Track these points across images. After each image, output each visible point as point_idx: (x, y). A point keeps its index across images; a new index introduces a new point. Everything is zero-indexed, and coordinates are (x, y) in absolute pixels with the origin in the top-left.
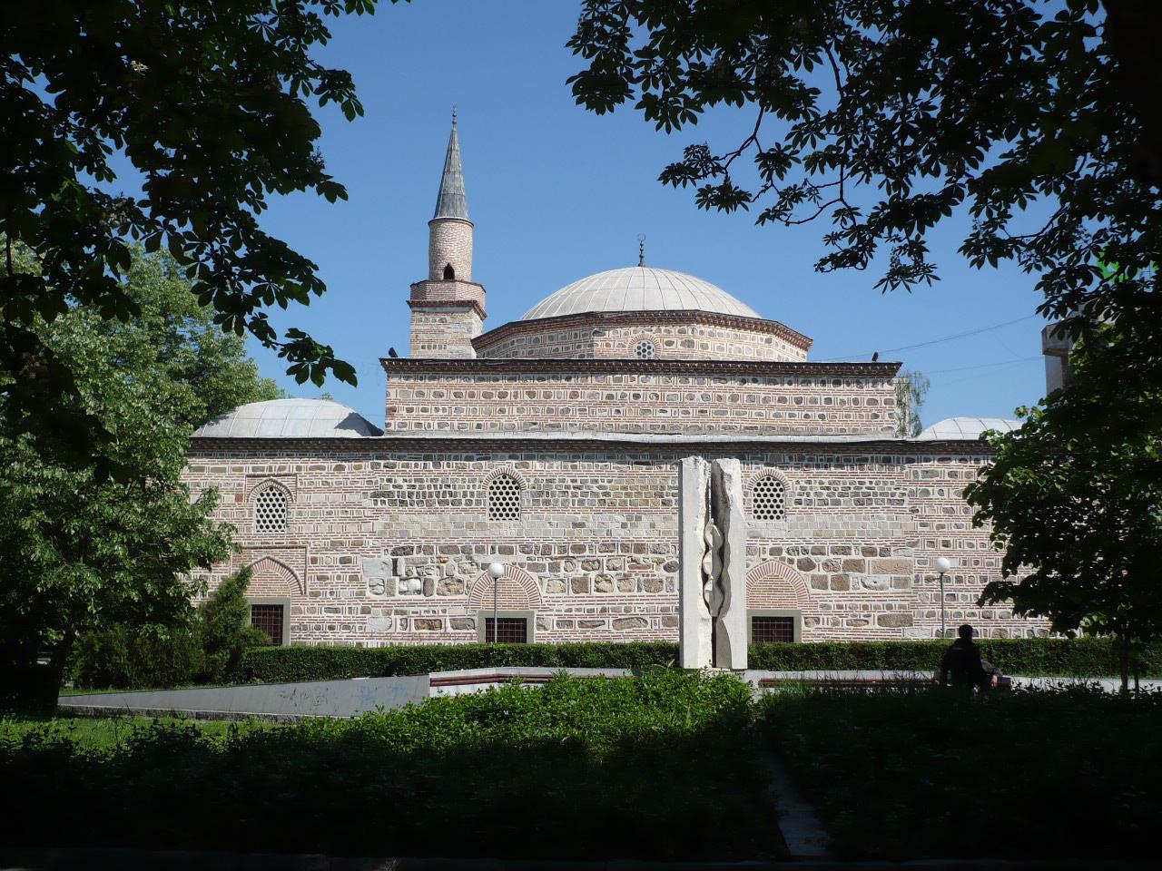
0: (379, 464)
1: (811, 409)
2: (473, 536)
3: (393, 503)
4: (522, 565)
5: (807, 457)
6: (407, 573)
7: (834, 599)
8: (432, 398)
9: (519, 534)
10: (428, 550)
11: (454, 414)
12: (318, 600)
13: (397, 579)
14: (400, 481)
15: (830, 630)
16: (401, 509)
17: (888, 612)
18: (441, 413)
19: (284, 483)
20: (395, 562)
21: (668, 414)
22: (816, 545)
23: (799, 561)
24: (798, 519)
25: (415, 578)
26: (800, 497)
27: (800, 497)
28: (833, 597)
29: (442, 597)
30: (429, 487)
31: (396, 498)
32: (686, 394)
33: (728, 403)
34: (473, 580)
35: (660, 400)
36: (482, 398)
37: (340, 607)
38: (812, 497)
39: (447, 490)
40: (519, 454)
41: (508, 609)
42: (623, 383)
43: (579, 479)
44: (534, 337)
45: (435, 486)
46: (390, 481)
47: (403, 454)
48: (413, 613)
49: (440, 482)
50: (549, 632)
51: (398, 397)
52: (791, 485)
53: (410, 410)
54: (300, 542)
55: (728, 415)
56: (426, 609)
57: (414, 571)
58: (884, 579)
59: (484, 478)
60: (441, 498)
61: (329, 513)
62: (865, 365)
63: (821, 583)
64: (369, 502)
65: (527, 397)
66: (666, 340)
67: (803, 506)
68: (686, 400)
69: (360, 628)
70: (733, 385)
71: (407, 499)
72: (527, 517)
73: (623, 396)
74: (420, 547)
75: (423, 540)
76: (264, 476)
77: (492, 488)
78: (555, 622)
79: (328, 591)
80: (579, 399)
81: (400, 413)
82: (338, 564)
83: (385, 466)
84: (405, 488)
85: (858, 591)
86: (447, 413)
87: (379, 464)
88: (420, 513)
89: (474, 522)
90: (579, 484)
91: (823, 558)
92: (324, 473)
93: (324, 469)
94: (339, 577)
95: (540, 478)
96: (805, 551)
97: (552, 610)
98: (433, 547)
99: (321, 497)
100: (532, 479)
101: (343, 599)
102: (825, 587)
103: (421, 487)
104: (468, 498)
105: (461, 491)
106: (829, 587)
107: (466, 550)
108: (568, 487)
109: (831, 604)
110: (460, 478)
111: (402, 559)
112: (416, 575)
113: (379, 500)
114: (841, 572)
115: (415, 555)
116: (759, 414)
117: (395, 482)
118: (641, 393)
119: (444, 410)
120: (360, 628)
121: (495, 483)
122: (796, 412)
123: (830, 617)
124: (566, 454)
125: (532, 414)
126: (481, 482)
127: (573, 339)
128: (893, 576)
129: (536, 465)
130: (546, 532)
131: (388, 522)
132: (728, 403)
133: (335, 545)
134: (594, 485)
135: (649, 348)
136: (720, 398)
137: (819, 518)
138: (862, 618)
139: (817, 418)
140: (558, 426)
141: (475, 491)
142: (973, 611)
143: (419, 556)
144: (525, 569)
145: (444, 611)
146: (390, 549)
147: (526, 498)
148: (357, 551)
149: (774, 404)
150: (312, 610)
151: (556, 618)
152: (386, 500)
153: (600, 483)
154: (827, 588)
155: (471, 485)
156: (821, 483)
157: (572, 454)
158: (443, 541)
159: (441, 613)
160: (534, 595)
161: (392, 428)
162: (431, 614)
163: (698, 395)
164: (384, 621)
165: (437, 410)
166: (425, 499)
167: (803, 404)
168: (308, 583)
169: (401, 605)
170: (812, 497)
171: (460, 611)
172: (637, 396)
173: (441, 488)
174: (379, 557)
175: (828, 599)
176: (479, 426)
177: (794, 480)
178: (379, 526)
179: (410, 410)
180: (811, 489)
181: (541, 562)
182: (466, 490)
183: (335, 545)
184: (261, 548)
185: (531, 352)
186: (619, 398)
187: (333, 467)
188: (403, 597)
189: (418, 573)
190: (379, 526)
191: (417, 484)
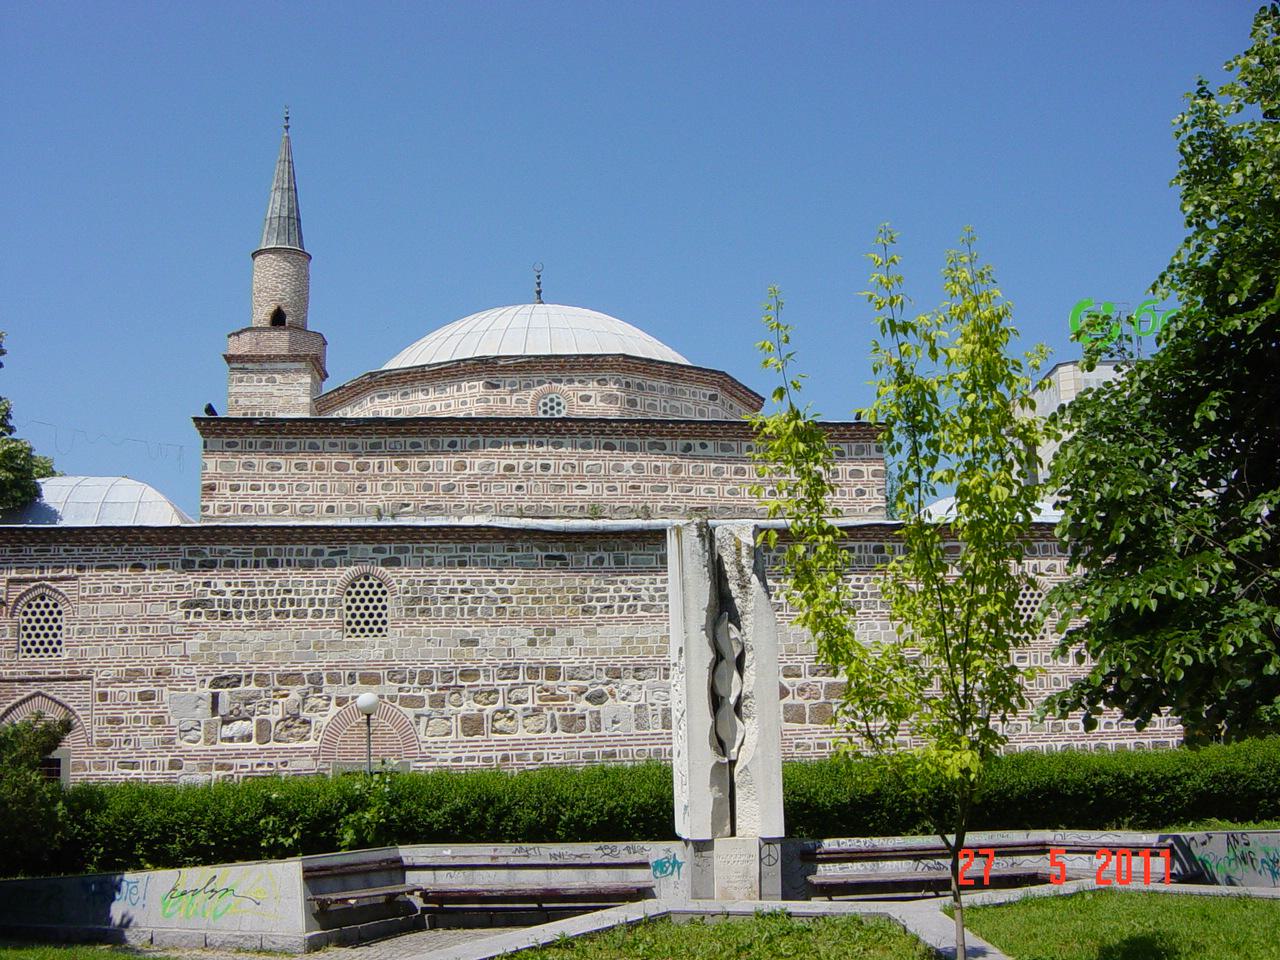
0: (193, 562)
3: (212, 615)
4: (392, 699)
7: (813, 736)
8: (265, 471)
9: (388, 654)
10: (262, 679)
11: (295, 492)
12: (109, 751)
14: (221, 585)
16: (224, 623)
18: (277, 491)
19: (61, 590)
20: (215, 697)
21: (588, 491)
22: (789, 664)
32: (612, 463)
33: (668, 476)
35: (576, 473)
36: (334, 471)
39: (287, 596)
40: (387, 546)
46: (207, 584)
48: (242, 767)
49: (276, 587)
54: (82, 670)
56: (259, 761)
60: (279, 608)
61: (124, 630)
62: (847, 425)
65: (396, 469)
66: (580, 394)
68: (612, 472)
72: (394, 635)
73: (528, 467)
74: (249, 676)
75: (255, 668)
76: (34, 580)
80: (467, 471)
81: (222, 491)
84: (228, 596)
86: (286, 492)
87: (193, 562)
90: (468, 585)
91: (799, 682)
94: (137, 719)
97: (434, 760)
99: (112, 608)
100: (405, 581)
102: (803, 721)
104: (317, 607)
107: (316, 681)
108: (454, 591)
109: (810, 742)
110: (305, 580)
113: (193, 611)
115: (242, 687)
117: (216, 586)
118: (551, 462)
119: (282, 487)
124: (451, 545)
125: (404, 491)
126: (334, 585)
132: (668, 476)
133: (133, 675)
135: (559, 404)
140: (437, 508)
143: (247, 688)
144: (396, 704)
146: (209, 679)
148: (162, 683)
149: (728, 476)
150: (101, 766)
152: (203, 611)
153: (498, 585)
157: (459, 546)
158: (282, 668)
161: (210, 512)
165: (272, 487)
169: (225, 756)
172: (545, 467)
176: (331, 509)
178: (194, 645)
182: (313, 596)
183: (133, 675)
184: (29, 680)
186: (521, 469)
188: (228, 745)
191: (246, 589)
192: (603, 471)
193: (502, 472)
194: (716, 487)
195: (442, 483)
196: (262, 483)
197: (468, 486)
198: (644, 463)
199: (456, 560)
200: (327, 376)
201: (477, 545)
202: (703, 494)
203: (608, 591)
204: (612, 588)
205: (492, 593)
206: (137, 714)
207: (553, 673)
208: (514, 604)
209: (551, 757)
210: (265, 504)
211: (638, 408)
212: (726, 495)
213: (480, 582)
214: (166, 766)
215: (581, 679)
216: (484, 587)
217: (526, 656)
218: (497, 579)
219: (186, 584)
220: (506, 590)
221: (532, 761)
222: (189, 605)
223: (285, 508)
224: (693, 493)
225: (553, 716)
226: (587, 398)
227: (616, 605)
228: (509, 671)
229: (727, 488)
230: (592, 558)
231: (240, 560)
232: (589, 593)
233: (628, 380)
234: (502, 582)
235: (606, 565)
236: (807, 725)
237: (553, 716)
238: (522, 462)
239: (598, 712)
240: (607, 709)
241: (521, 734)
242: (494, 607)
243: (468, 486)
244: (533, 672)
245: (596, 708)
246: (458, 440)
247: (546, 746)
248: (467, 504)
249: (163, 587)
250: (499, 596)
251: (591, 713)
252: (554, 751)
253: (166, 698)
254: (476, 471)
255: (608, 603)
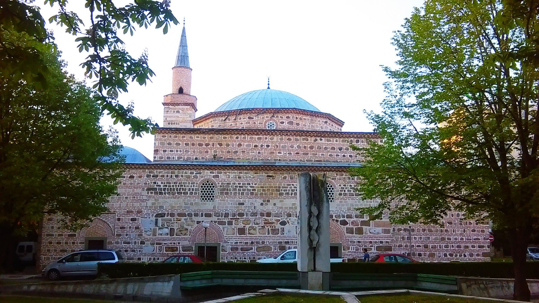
1: (346, 153)
2: (192, 209)
3: (156, 193)
4: (215, 222)
5: (344, 174)
6: (162, 226)
8: (175, 145)
9: (214, 207)
10: (172, 215)
11: (185, 153)
12: (120, 238)
13: (157, 228)
14: (160, 183)
15: (355, 252)
16: (160, 196)
17: (381, 245)
18: (179, 152)
20: (157, 220)
21: (282, 154)
22: (348, 214)
23: (340, 221)
24: (340, 202)
25: (166, 228)
26: (341, 192)
27: (341, 192)
28: (356, 237)
29: (178, 237)
30: (173, 186)
31: (158, 191)
32: (290, 145)
33: (309, 150)
34: (193, 229)
35: (278, 148)
36: (198, 146)
37: (131, 241)
38: (346, 192)
39: (181, 188)
40: (215, 171)
41: (211, 241)
42: (262, 140)
43: (241, 183)
44: (221, 119)
45: (176, 186)
46: (155, 183)
47: (161, 171)
48: (164, 244)
49: (178, 184)
50: (227, 253)
51: (160, 145)
52: (337, 186)
53: (165, 151)
55: (309, 155)
56: (170, 242)
57: (166, 224)
58: (380, 229)
59: (198, 182)
60: (178, 191)
61: (126, 198)
62: (370, 133)
63: (350, 231)
64: (145, 193)
66: (281, 121)
67: (342, 196)
68: (290, 148)
69: (140, 251)
70: (311, 140)
71: (163, 191)
72: (217, 200)
73: (262, 146)
75: (170, 210)
77: (202, 187)
78: (230, 248)
79: (125, 234)
80: (242, 147)
82: (130, 221)
83: (153, 177)
84: (162, 187)
85: (367, 235)
86: (182, 153)
87: (150, 175)
88: (169, 198)
89: (194, 202)
90: (241, 185)
91: (352, 220)
92: (124, 179)
93: (125, 178)
94: (130, 227)
95: (224, 182)
96: (344, 217)
97: (229, 243)
98: (174, 213)
100: (220, 183)
101: (132, 238)
103: (169, 186)
104: (191, 191)
105: (188, 188)
106: (354, 233)
107: (190, 215)
108: (236, 187)
110: (187, 182)
111: (160, 219)
112: (166, 226)
113: (150, 192)
114: (359, 226)
115: (166, 217)
116: (323, 154)
117: (158, 184)
118: (270, 145)
119: (180, 151)
120: (140, 251)
121: (203, 184)
122: (339, 154)
123: (355, 246)
124: (236, 171)
126: (197, 184)
127: (239, 120)
128: (383, 228)
129: (222, 176)
130: (227, 207)
131: (154, 202)
132: (309, 150)
134: (249, 186)
135: (273, 124)
136: (305, 147)
137: (350, 202)
138: (369, 247)
139: (349, 157)
141: (194, 188)
142: (419, 244)
143: (167, 218)
144: (217, 224)
145: (179, 243)
146: (155, 215)
147: (217, 192)
148: (139, 215)
149: (329, 150)
151: (230, 246)
152: (153, 192)
153: (251, 185)
154: (353, 234)
155: (192, 185)
156: (350, 186)
157: (238, 172)
158: (179, 211)
159: (177, 244)
160: (220, 236)
161: (156, 159)
162: (173, 244)
163: (295, 146)
164: (151, 248)
165: (177, 151)
166: (171, 192)
167: (342, 150)
168: (116, 230)
170: (346, 192)
171: (186, 243)
172: (268, 146)
173: (179, 187)
174: (149, 218)
175: (354, 238)
176: (196, 159)
177: (339, 184)
178: (149, 203)
179: (165, 151)
180: (346, 188)
181: (224, 221)
182: (190, 187)
185: (220, 126)
186: (260, 146)
187: (129, 177)
188: (160, 236)
189: (167, 225)
190: (149, 203)
191: (168, 185)
192: (287, 148)
193: (253, 147)
194: (325, 154)
195: (233, 151)
196: (174, 150)
197: (242, 152)
198: (301, 145)
199: (237, 176)
200: (197, 110)
201: (245, 171)
202: (320, 156)
203: (288, 188)
204: (289, 187)
205: (249, 188)
206: (130, 226)
207: (269, 215)
208: (256, 191)
209: (267, 243)
210: (175, 156)
211: (300, 126)
212: (328, 156)
213: (245, 184)
214: (140, 243)
215: (278, 217)
216: (246, 185)
217: (260, 208)
218: (251, 183)
219: (148, 183)
220: (254, 187)
221: (261, 244)
222: (148, 189)
223: (182, 158)
224: (317, 155)
225: (268, 229)
226: (282, 123)
227: (290, 192)
228: (254, 214)
229: (329, 154)
230: (282, 177)
231: (166, 175)
232: (281, 188)
233: (297, 116)
234: (252, 184)
235: (287, 179)
236: (354, 235)
237: (268, 229)
238: (260, 144)
239: (284, 228)
240: (286, 227)
241: (258, 235)
242: (250, 192)
243: (242, 152)
244: (262, 215)
245: (283, 227)
246: (239, 136)
247: (266, 239)
248: (241, 158)
249: (140, 184)
250: (251, 189)
251: (281, 228)
252: (268, 241)
253: (140, 221)
254: (245, 147)
255: (287, 192)
